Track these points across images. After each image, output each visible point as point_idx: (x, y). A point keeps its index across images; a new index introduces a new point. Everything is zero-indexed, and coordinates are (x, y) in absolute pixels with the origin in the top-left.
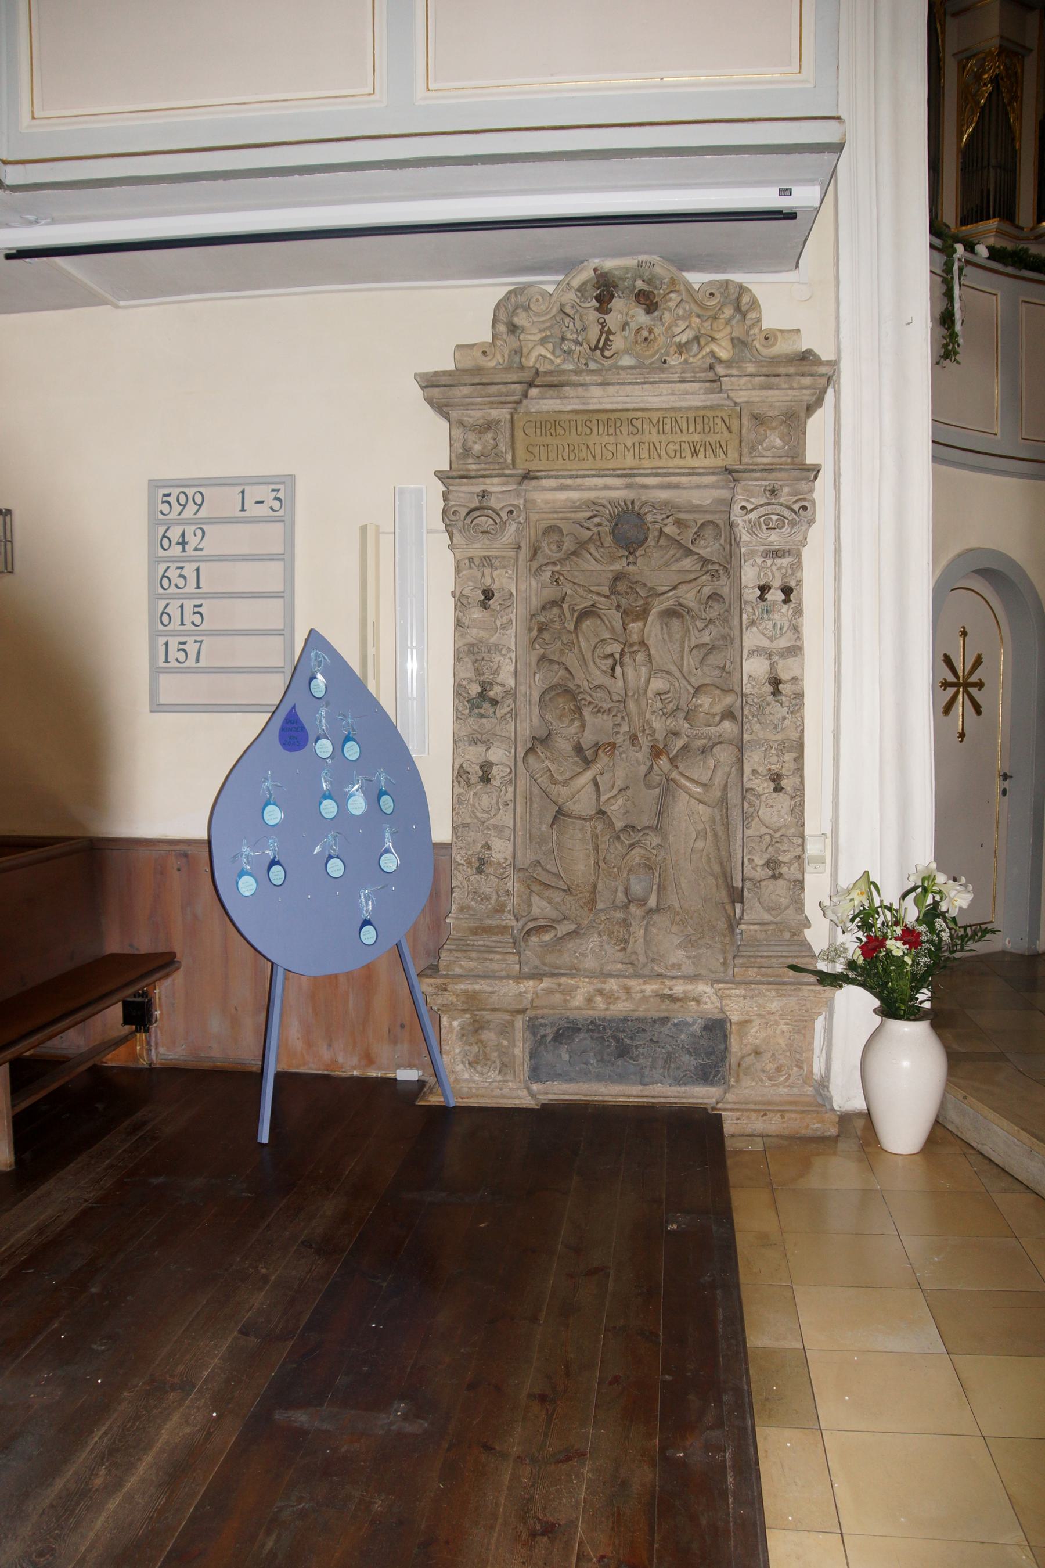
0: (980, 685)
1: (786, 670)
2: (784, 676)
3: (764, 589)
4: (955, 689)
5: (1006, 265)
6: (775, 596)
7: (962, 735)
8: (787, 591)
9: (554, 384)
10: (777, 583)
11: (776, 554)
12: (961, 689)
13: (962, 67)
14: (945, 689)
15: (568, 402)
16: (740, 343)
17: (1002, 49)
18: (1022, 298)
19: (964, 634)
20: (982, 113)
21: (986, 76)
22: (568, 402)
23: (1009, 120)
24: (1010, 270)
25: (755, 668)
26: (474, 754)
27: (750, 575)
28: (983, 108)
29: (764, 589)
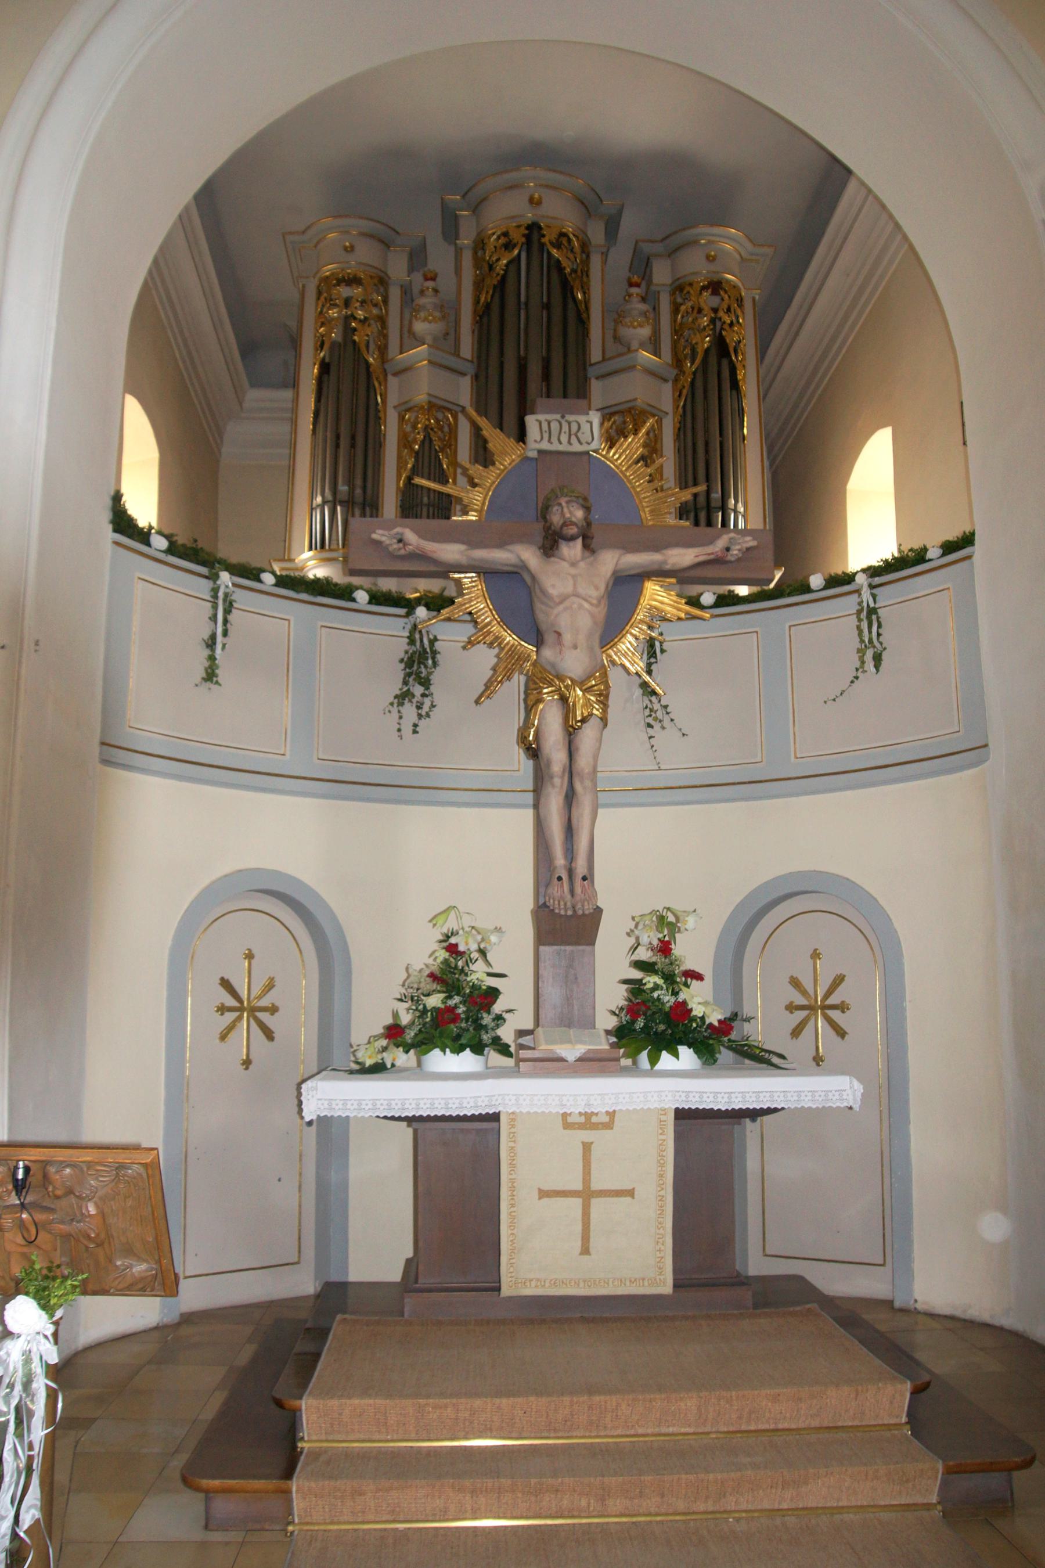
0: (222, 1009)
4: (234, 1015)
5: (298, 592)
7: (247, 1063)
12: (245, 1015)
13: (402, 418)
14: (222, 1014)
18: (321, 623)
19: (250, 956)
20: (417, 460)
21: (419, 426)
23: (442, 466)
24: (304, 596)
28: (417, 453)
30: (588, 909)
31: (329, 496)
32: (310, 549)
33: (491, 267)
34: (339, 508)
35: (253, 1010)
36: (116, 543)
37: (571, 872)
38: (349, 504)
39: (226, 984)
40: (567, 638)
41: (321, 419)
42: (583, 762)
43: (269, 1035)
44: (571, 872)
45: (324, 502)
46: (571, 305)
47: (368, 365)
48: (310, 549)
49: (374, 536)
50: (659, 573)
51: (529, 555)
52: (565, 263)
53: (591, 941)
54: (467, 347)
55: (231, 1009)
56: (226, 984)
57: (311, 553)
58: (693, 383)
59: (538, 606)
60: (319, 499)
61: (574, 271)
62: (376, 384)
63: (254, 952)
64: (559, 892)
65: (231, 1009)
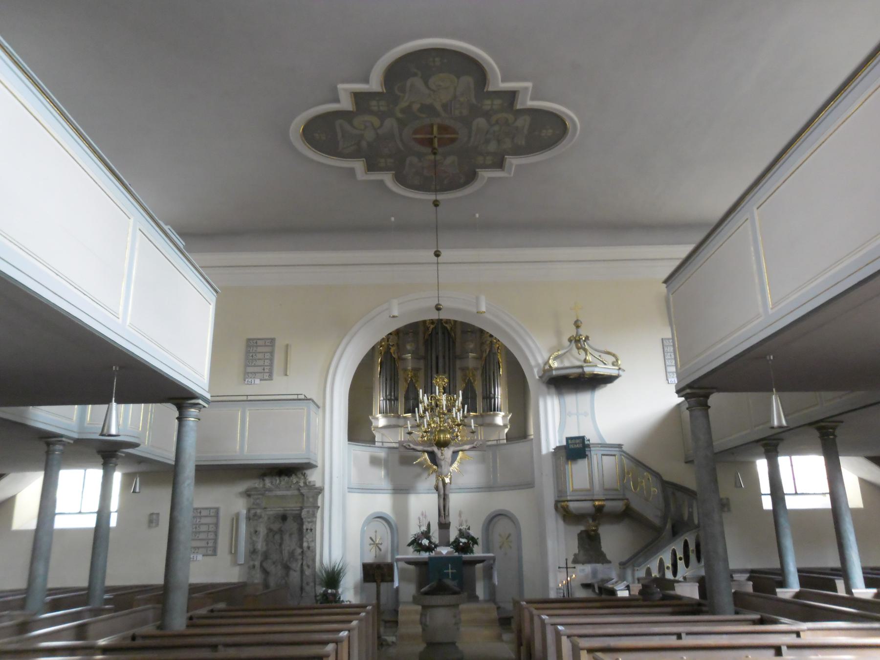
1: (312, 545)
2: (311, 545)
3: (307, 529)
6: (309, 531)
8: (311, 530)
9: (270, 490)
10: (309, 528)
11: (309, 522)
15: (274, 493)
16: (305, 483)
17: (412, 369)
22: (274, 493)
25: (305, 545)
26: (251, 563)
27: (305, 527)
29: (307, 529)
30: (448, 522)
31: (385, 398)
32: (380, 413)
33: (428, 329)
34: (388, 401)
35: (377, 544)
36: (349, 444)
37: (445, 514)
38: (390, 400)
39: (371, 538)
40: (443, 467)
41: (382, 374)
42: (447, 492)
43: (380, 550)
44: (445, 514)
45: (384, 399)
46: (451, 340)
47: (394, 358)
48: (380, 413)
49: (404, 445)
50: (462, 450)
51: (435, 449)
52: (449, 328)
53: (449, 529)
54: (422, 352)
55: (373, 544)
56: (371, 538)
57: (381, 415)
58: (486, 360)
59: (437, 460)
60: (382, 398)
61: (451, 328)
62: (397, 364)
63: (377, 530)
64: (443, 521)
65: (373, 544)
